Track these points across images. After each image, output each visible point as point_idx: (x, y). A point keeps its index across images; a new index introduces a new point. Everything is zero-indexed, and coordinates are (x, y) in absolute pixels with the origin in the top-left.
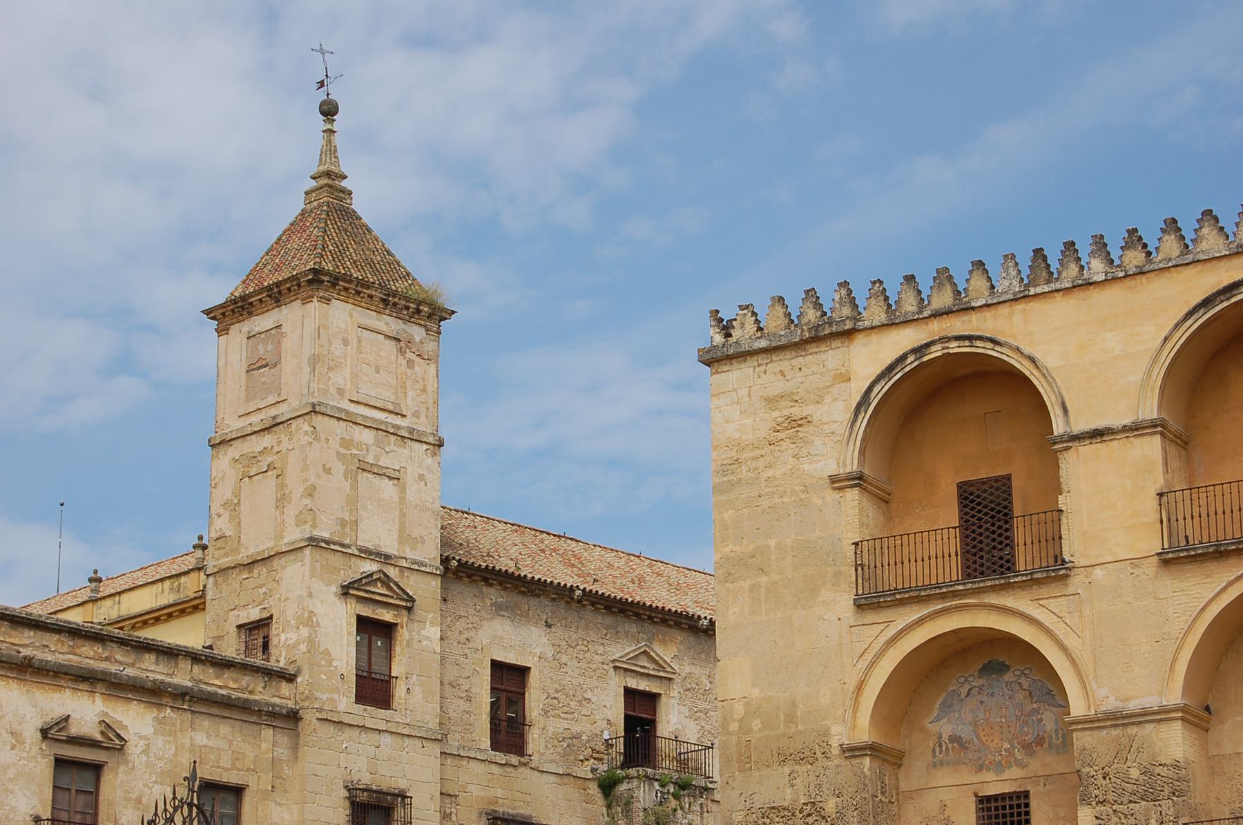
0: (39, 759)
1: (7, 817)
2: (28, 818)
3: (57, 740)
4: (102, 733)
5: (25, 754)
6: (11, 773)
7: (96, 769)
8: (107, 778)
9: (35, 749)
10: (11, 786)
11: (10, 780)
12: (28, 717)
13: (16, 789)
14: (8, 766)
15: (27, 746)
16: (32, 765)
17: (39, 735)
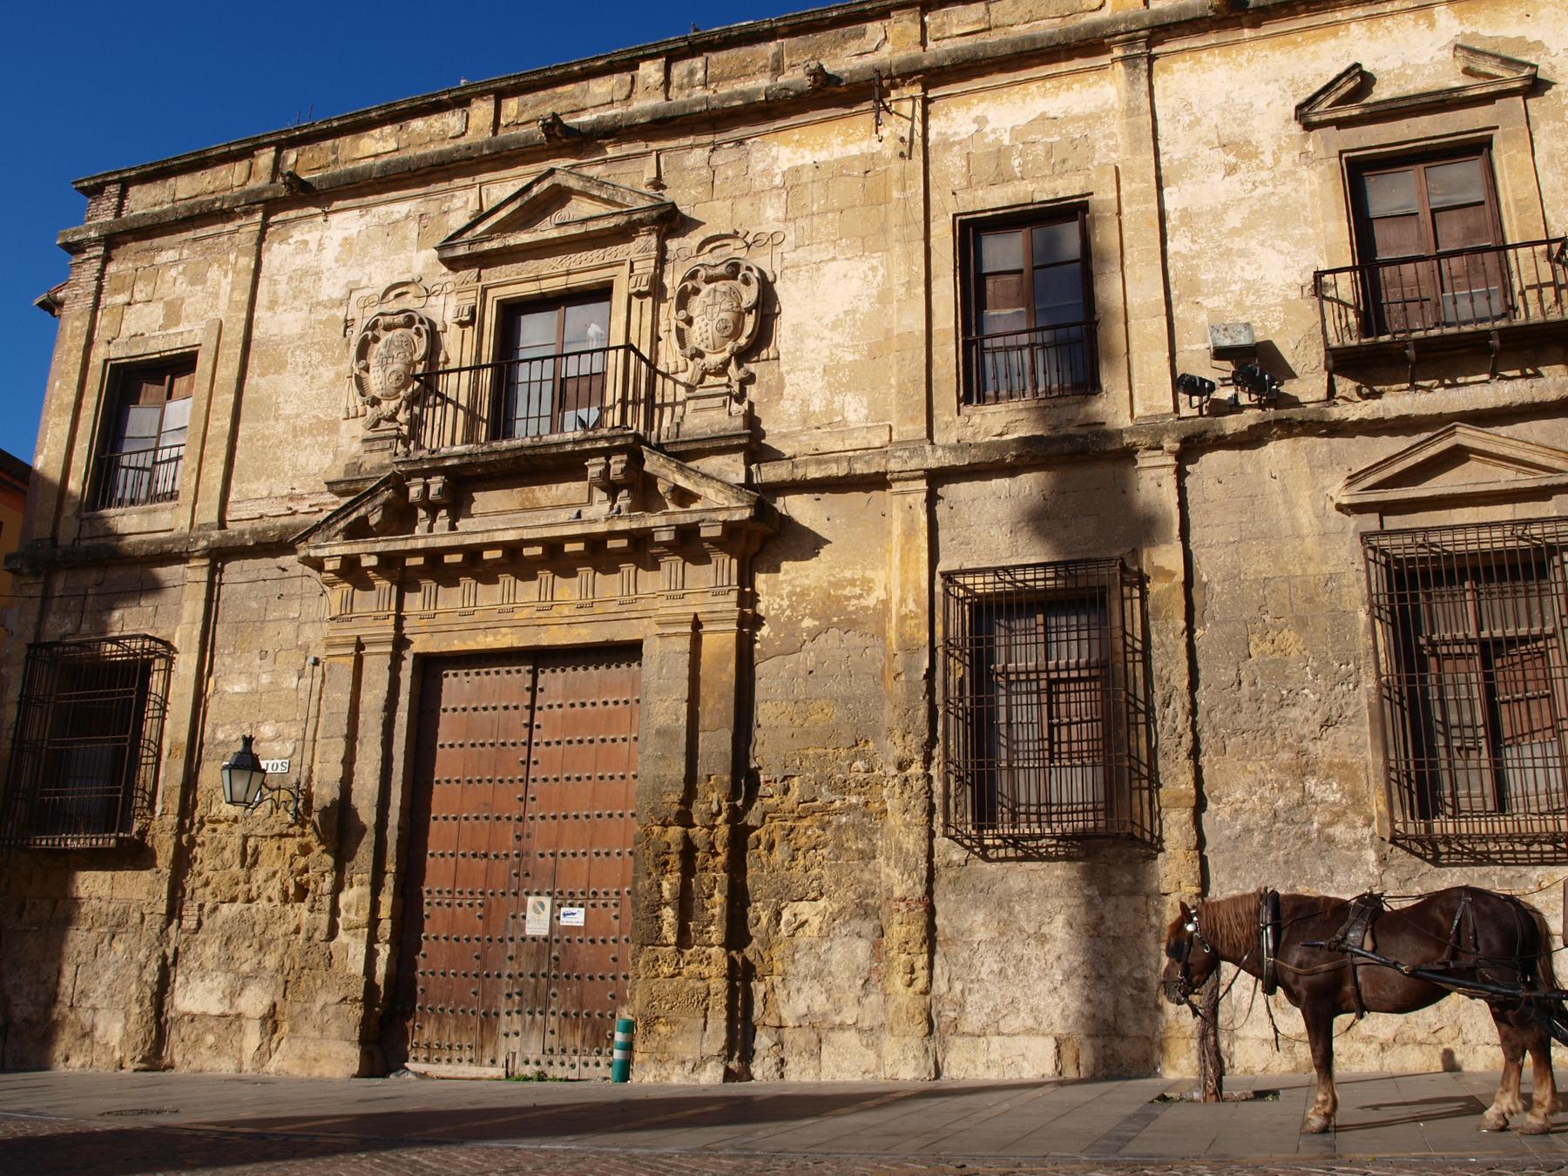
0: (1304, 172)
1: (1239, 304)
2: (1294, 295)
3: (1341, 124)
4: (1468, 71)
5: (1264, 175)
6: (1234, 220)
7: (1477, 147)
8: (1506, 157)
9: (1286, 161)
10: (1237, 243)
11: (1235, 232)
12: (1260, 104)
13: (1253, 244)
14: (1226, 207)
15: (1268, 159)
16: (1287, 188)
17: (1296, 128)
